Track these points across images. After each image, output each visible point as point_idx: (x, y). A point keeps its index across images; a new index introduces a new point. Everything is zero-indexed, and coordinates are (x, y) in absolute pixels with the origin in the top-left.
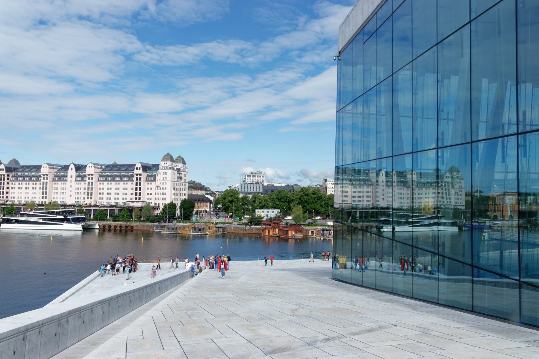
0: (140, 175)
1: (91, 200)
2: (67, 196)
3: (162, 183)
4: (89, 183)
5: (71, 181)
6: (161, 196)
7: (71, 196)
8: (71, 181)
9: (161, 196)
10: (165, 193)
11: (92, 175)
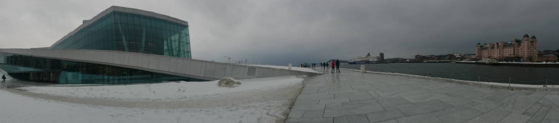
2: (495, 54)
9: (523, 53)
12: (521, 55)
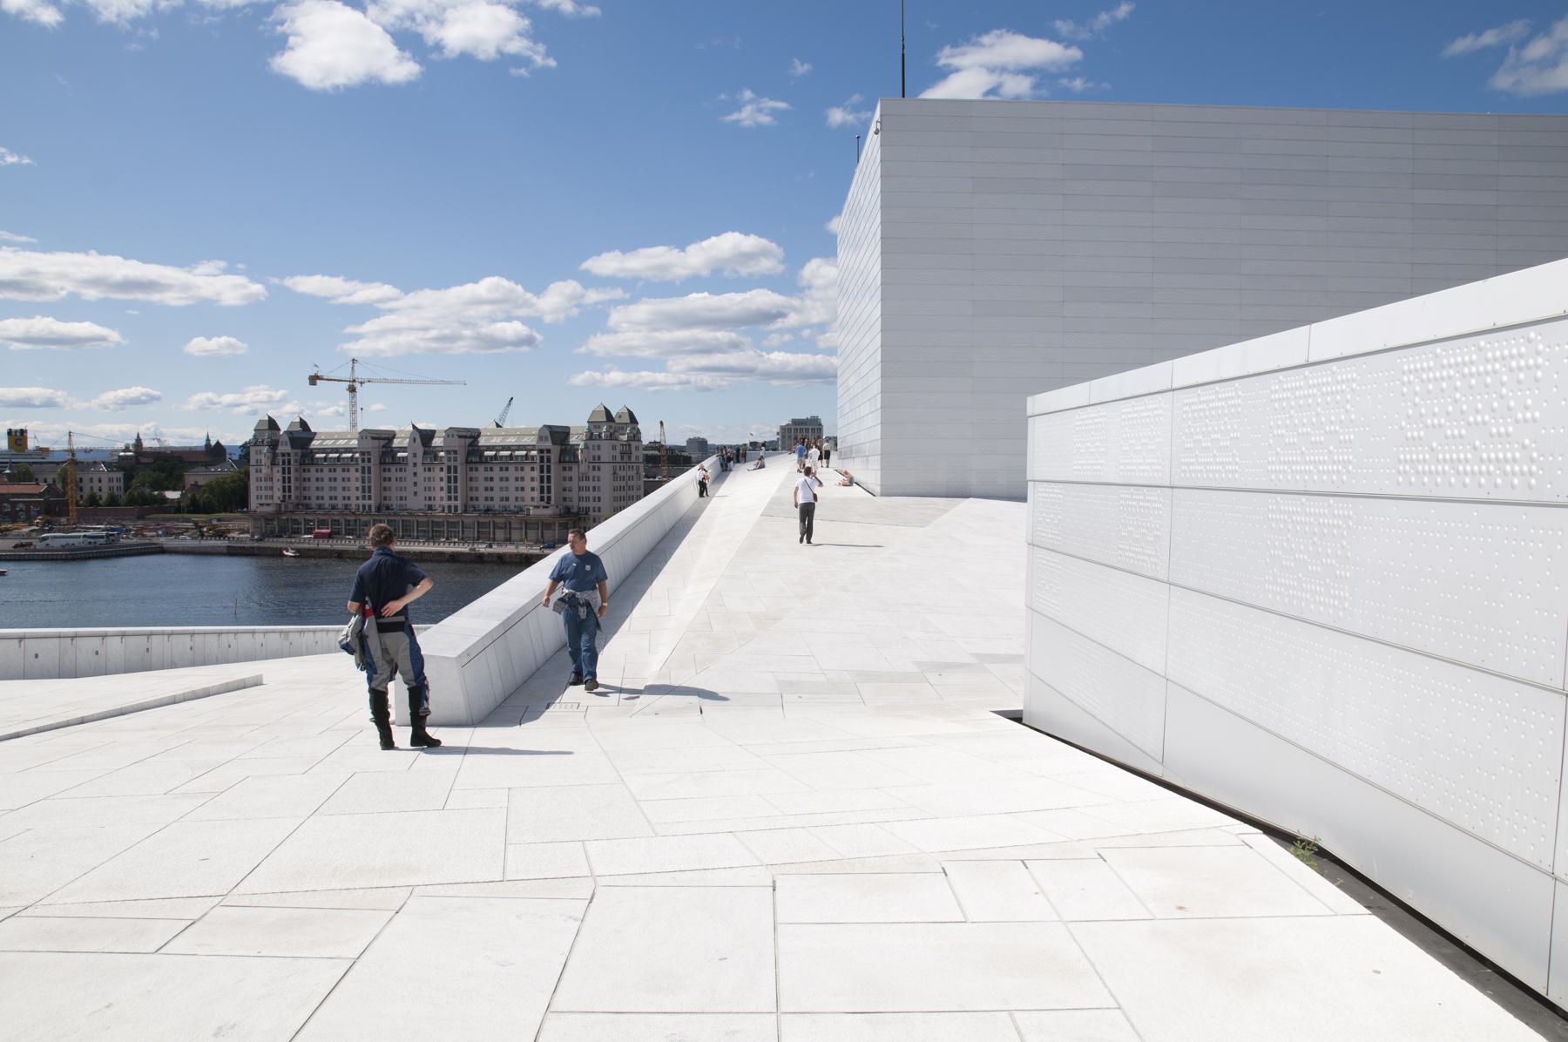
0: (549, 451)
1: (456, 503)
2: (409, 494)
3: (591, 468)
4: (449, 468)
5: (415, 464)
6: (591, 494)
7: (415, 493)
8: (415, 464)
10: (599, 487)
11: (456, 452)
12: (584, 504)
